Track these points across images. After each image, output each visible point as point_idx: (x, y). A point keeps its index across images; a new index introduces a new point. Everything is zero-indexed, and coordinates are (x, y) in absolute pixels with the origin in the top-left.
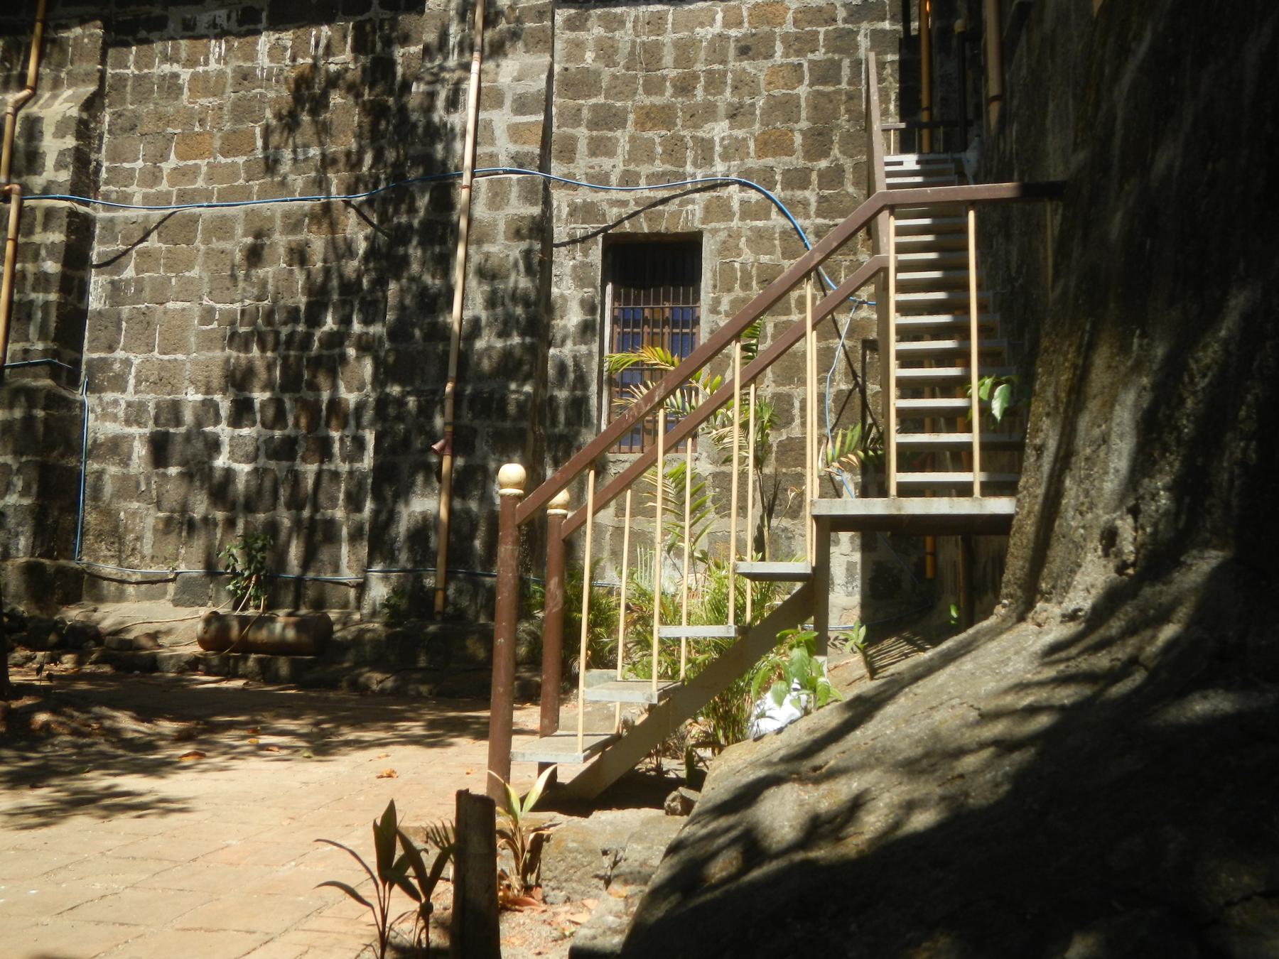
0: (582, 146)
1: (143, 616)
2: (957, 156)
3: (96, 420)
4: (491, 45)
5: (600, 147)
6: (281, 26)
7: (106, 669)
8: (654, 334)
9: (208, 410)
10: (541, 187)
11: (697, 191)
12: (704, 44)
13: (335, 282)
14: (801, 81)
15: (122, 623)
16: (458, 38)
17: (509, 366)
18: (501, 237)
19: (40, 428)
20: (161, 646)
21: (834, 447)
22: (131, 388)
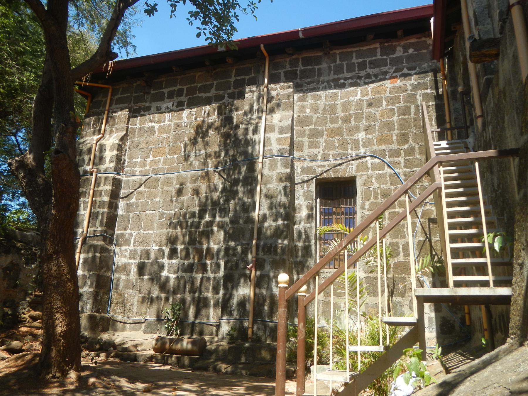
0: (306, 145)
1: (132, 338)
2: (464, 140)
4: (270, 109)
5: (313, 145)
6: (191, 107)
7: (117, 360)
8: (338, 218)
9: (161, 251)
10: (290, 161)
11: (353, 160)
12: (353, 103)
13: (209, 201)
14: (394, 115)
15: (123, 340)
16: (257, 107)
17: (278, 233)
18: (274, 181)
20: (138, 351)
21: (419, 265)
22: (132, 244)
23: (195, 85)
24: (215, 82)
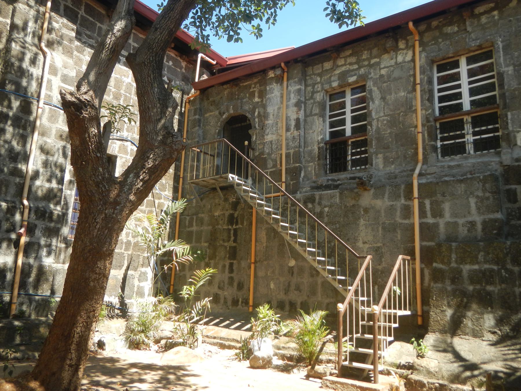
12: (125, 84)
16: (32, 30)
18: (53, 136)
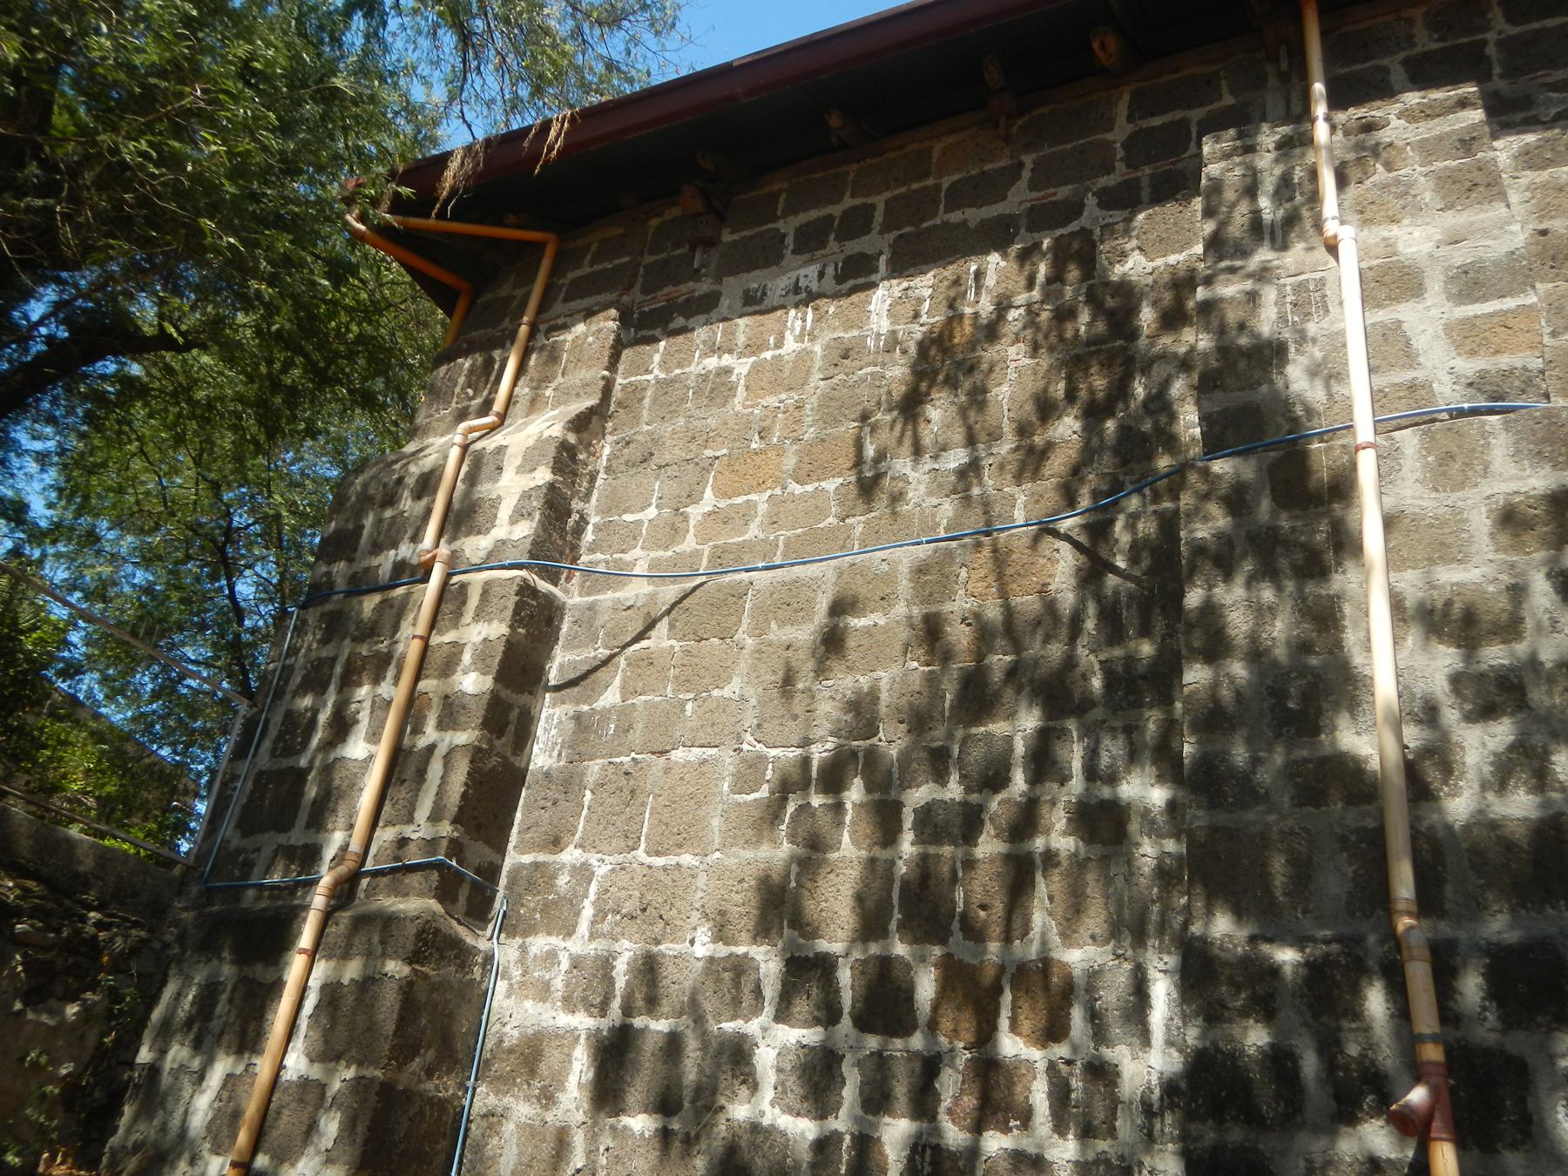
3: (508, 996)
6: (911, 271)
19: (389, 1002)
22: (583, 927)
23: (930, 182)
24: (1028, 160)
